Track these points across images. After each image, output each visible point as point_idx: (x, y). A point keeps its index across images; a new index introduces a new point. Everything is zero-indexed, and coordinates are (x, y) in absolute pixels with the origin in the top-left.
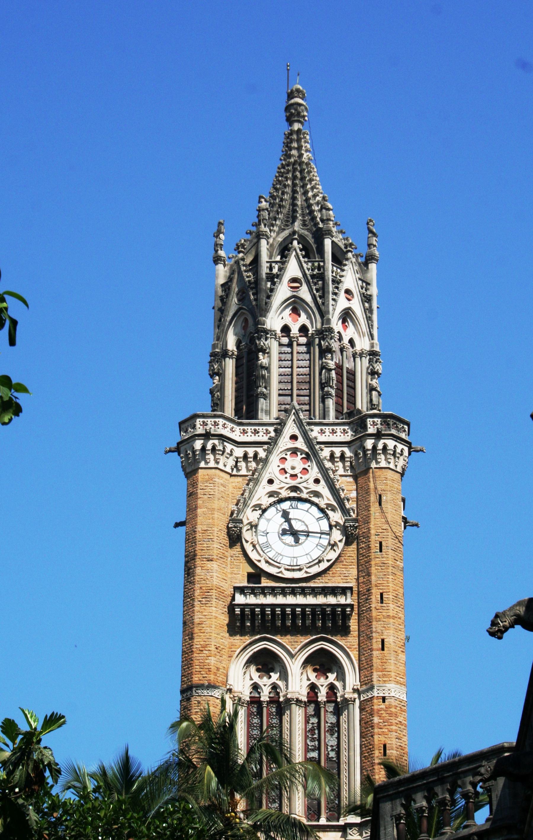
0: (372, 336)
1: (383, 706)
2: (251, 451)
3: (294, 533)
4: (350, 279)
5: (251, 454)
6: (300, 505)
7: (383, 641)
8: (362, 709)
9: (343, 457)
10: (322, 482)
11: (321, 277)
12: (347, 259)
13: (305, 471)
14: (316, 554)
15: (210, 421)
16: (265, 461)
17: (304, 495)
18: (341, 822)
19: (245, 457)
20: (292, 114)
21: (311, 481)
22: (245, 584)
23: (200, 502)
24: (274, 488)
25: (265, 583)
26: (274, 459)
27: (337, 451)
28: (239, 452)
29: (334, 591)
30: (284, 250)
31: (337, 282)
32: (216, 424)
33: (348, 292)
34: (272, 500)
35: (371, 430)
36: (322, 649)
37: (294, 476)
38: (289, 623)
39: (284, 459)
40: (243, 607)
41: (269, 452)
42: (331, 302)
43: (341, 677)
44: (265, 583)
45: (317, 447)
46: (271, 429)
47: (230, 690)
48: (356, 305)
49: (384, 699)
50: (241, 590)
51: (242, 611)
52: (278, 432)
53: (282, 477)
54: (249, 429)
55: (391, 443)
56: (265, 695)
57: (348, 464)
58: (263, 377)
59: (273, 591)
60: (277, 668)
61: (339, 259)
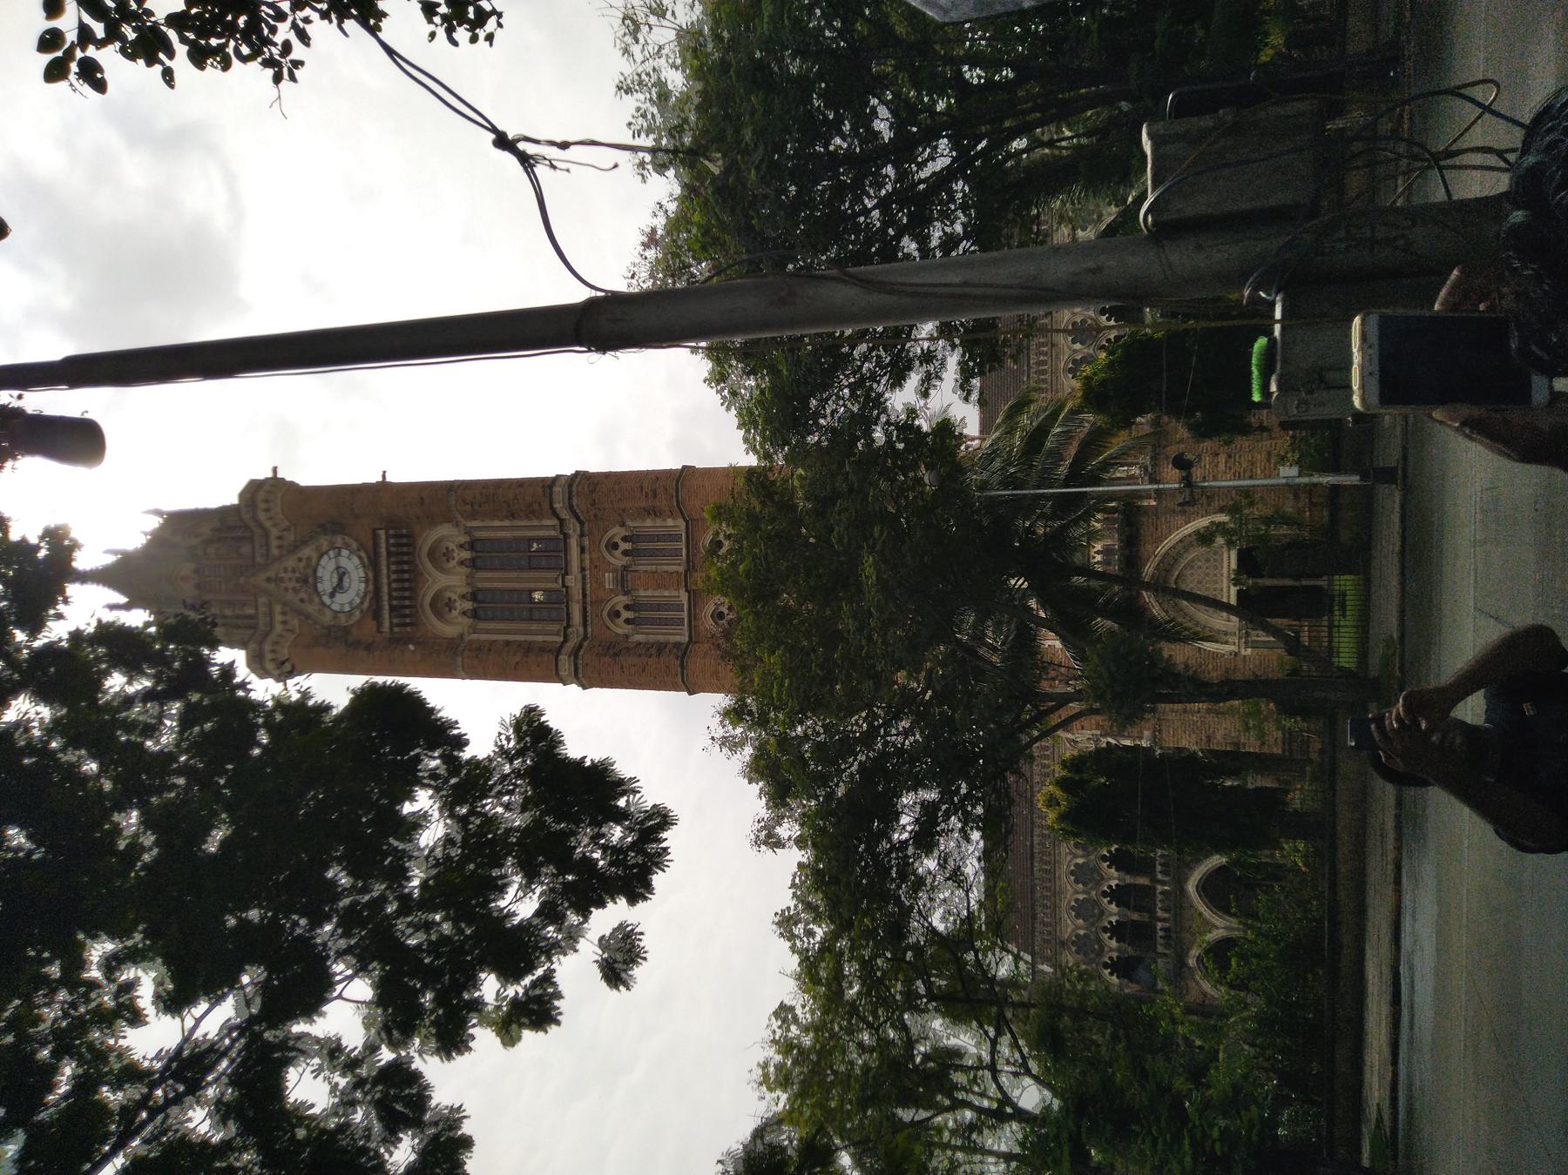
2: (278, 618)
3: (341, 580)
6: (319, 574)
9: (280, 538)
10: (300, 555)
13: (293, 571)
14: (356, 561)
16: (285, 604)
17: (310, 571)
19: (284, 622)
21: (302, 565)
27: (275, 543)
28: (279, 628)
29: (376, 545)
34: (316, 600)
39: (286, 589)
47: (462, 636)
50: (379, 625)
56: (468, 605)
60: (448, 594)
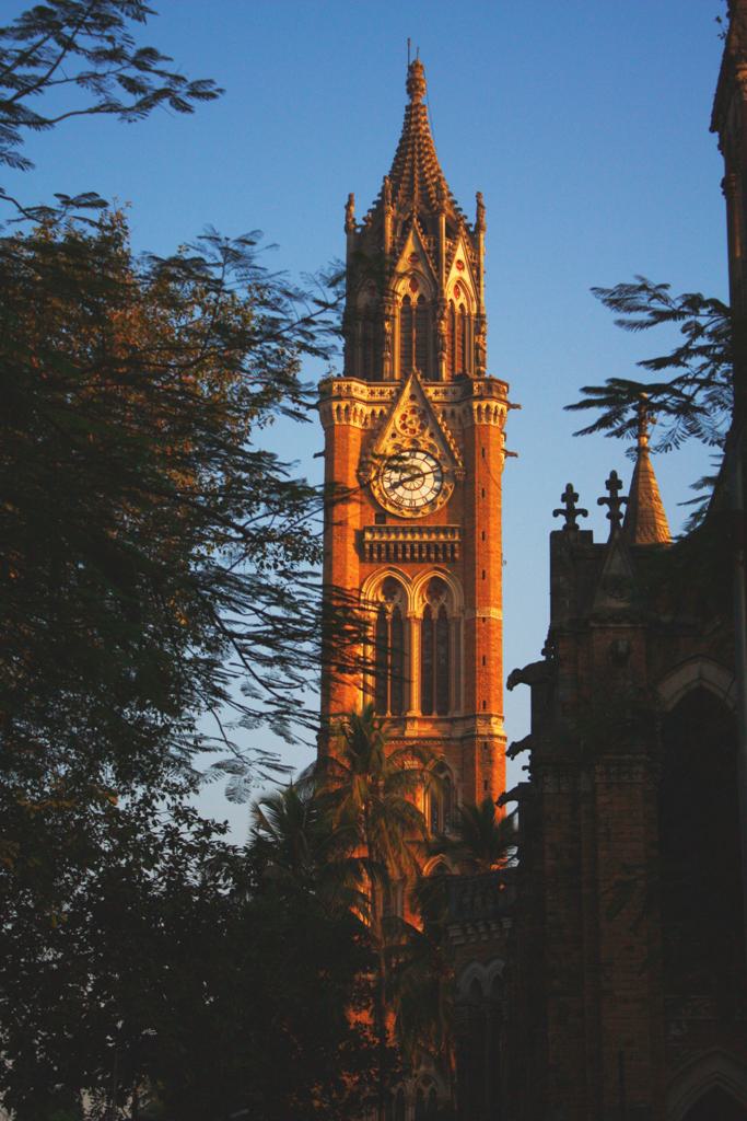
0: (478, 301)
1: (483, 625)
4: (460, 254)
5: (378, 412)
7: (484, 572)
8: (466, 627)
11: (437, 254)
12: (458, 233)
15: (344, 385)
18: (449, 716)
20: (413, 87)
22: (373, 524)
23: (336, 454)
24: (398, 440)
25: (390, 523)
26: (397, 416)
30: (405, 228)
31: (450, 256)
32: (349, 388)
33: (459, 262)
35: (476, 393)
36: (435, 577)
37: (413, 431)
38: (408, 555)
40: (372, 543)
41: (391, 411)
42: (445, 275)
43: (450, 599)
44: (390, 523)
45: (431, 405)
46: (393, 389)
48: (466, 275)
49: (484, 619)
50: (371, 530)
51: (371, 546)
52: (400, 393)
53: (403, 432)
54: (377, 389)
55: (493, 404)
57: (457, 421)
58: (388, 343)
59: (396, 531)
61: (452, 233)
